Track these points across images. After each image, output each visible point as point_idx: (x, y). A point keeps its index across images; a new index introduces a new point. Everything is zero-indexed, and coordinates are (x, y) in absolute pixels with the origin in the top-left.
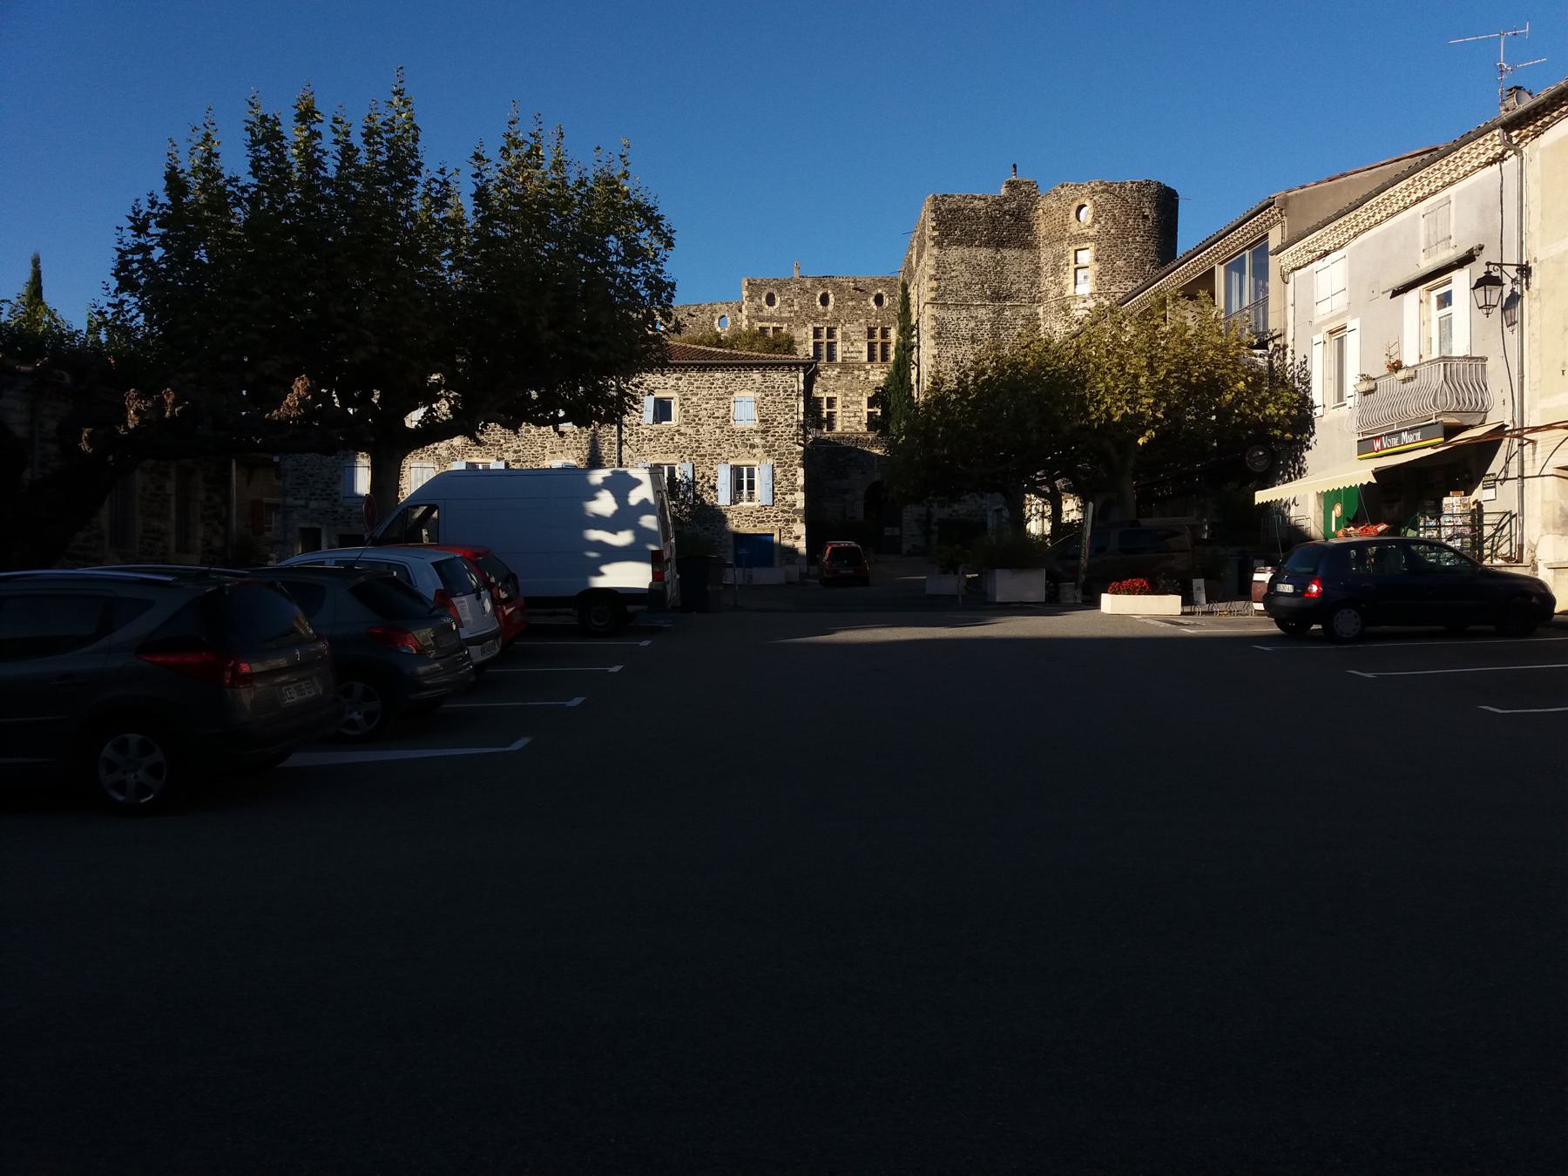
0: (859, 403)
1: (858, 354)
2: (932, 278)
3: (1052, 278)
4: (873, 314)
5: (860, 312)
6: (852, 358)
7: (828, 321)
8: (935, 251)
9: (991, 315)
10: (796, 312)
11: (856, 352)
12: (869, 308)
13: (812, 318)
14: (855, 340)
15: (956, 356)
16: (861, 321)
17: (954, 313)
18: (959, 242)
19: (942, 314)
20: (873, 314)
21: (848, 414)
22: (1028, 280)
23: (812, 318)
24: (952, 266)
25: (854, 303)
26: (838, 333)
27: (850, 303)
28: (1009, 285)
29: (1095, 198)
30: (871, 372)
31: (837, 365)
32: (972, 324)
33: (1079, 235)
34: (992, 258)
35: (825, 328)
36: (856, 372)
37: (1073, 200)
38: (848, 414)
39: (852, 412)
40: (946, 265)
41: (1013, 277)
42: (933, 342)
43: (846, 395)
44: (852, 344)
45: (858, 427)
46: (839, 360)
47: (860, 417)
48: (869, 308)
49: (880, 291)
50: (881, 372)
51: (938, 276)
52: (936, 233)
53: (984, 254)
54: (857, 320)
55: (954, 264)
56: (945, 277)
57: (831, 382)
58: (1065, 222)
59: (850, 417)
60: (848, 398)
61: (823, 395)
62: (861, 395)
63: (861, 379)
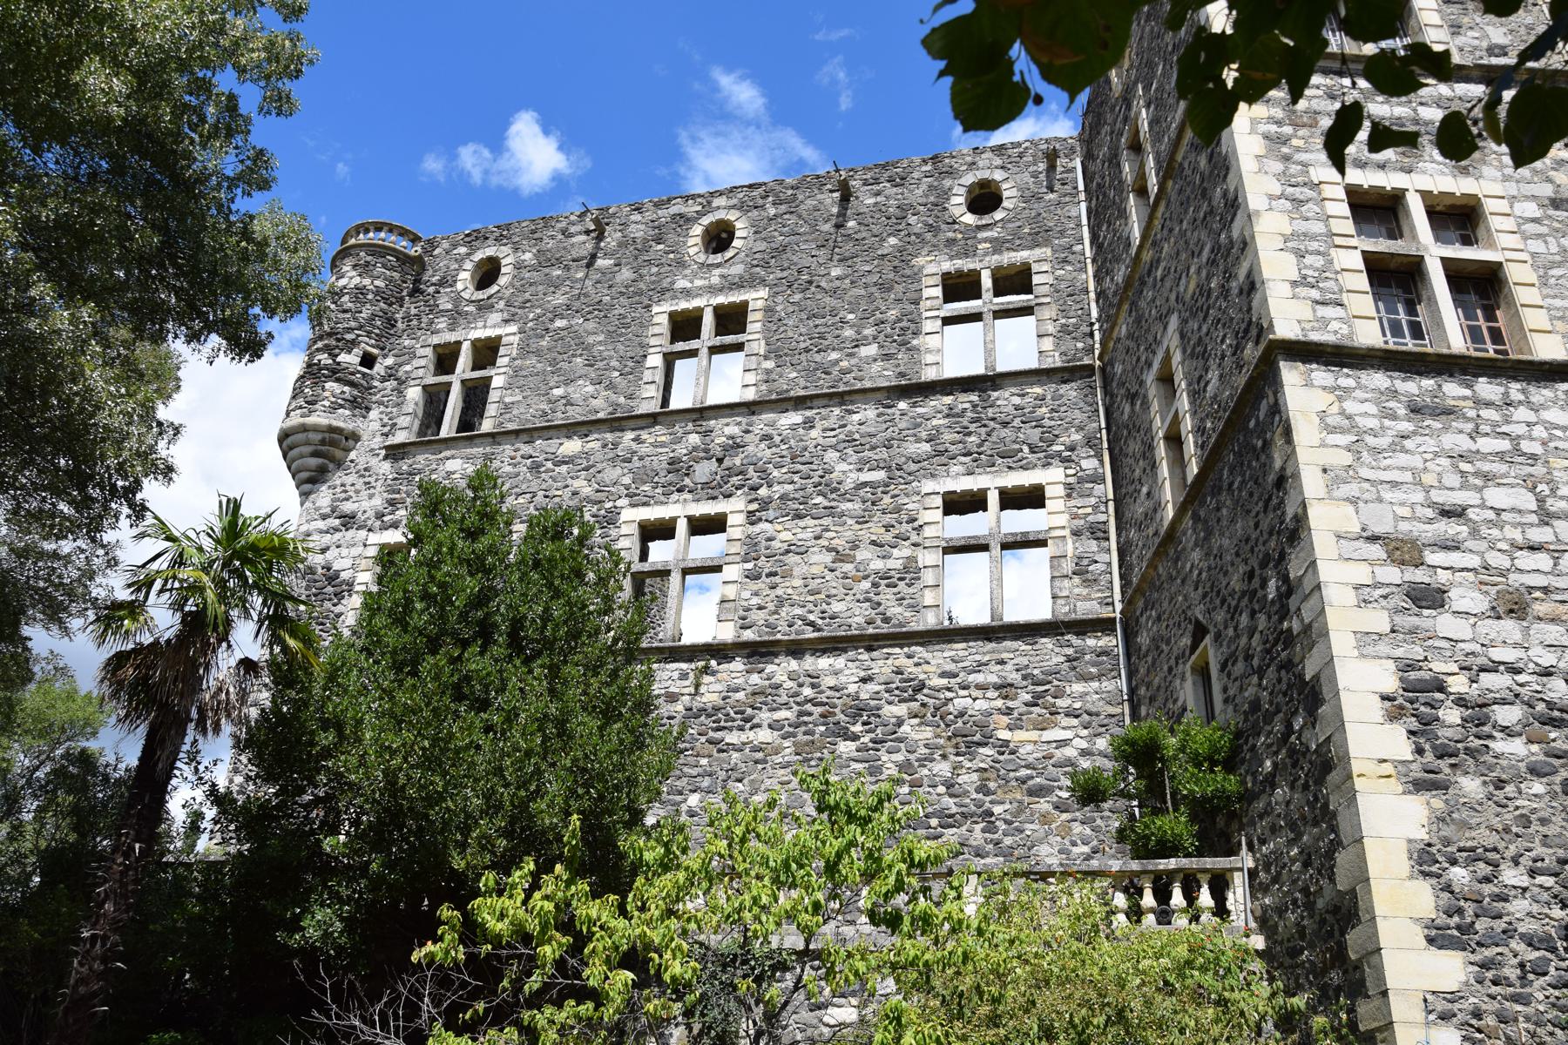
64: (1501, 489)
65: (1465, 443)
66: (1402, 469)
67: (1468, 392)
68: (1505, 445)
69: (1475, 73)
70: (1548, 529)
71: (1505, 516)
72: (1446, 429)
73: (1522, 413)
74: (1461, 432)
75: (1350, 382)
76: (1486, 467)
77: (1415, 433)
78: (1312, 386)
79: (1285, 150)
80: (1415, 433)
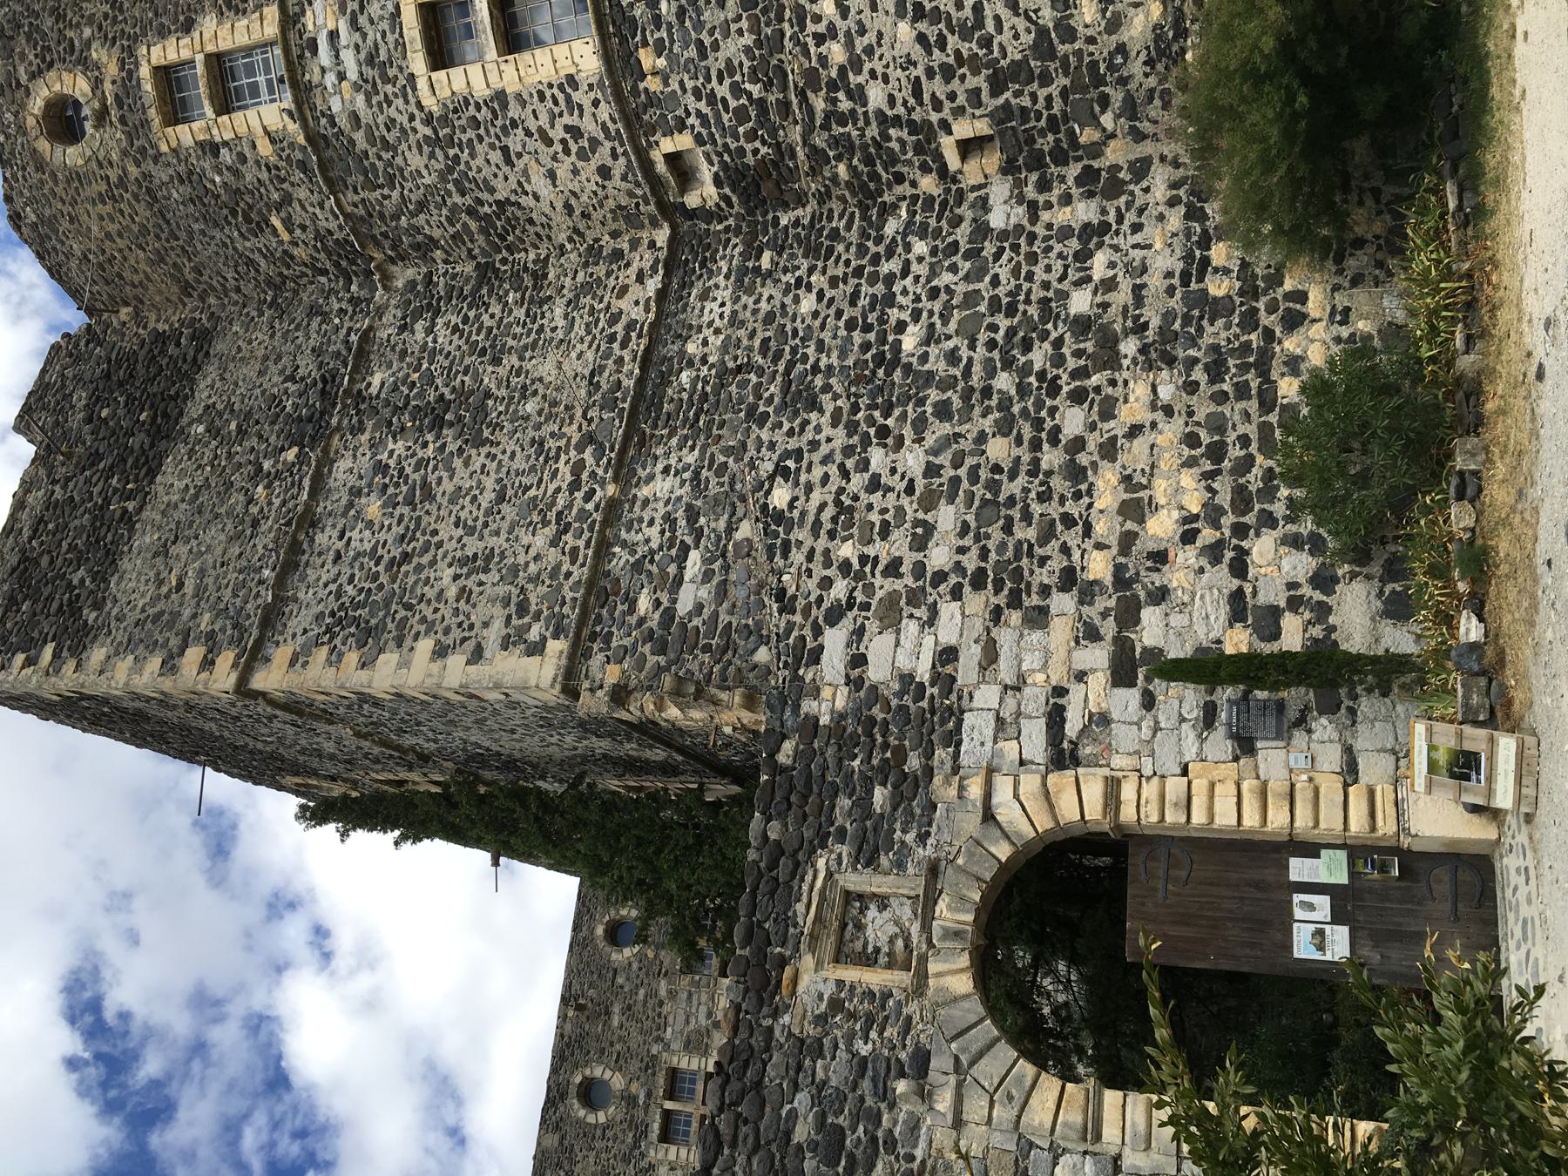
2: (170, 666)
3: (276, 221)
4: (651, 954)
5: (642, 992)
7: (649, 1095)
8: (97, 655)
9: (365, 438)
12: (635, 966)
13: (636, 1145)
14: (709, 1015)
15: (464, 561)
16: (663, 987)
17: (312, 578)
18: (107, 561)
19: (300, 620)
20: (651, 954)
22: (297, 329)
23: (636, 1145)
24: (164, 590)
25: (616, 1009)
27: (615, 1022)
28: (292, 388)
29: (23, 78)
32: (373, 507)
33: (123, 120)
34: (191, 452)
35: (669, 1105)
37: (40, 166)
40: (151, 611)
41: (274, 381)
42: (388, 660)
48: (635, 966)
49: (600, 930)
51: (174, 642)
52: (48, 652)
53: (173, 480)
54: (661, 1004)
55: (161, 583)
56: (187, 613)
58: (103, 187)
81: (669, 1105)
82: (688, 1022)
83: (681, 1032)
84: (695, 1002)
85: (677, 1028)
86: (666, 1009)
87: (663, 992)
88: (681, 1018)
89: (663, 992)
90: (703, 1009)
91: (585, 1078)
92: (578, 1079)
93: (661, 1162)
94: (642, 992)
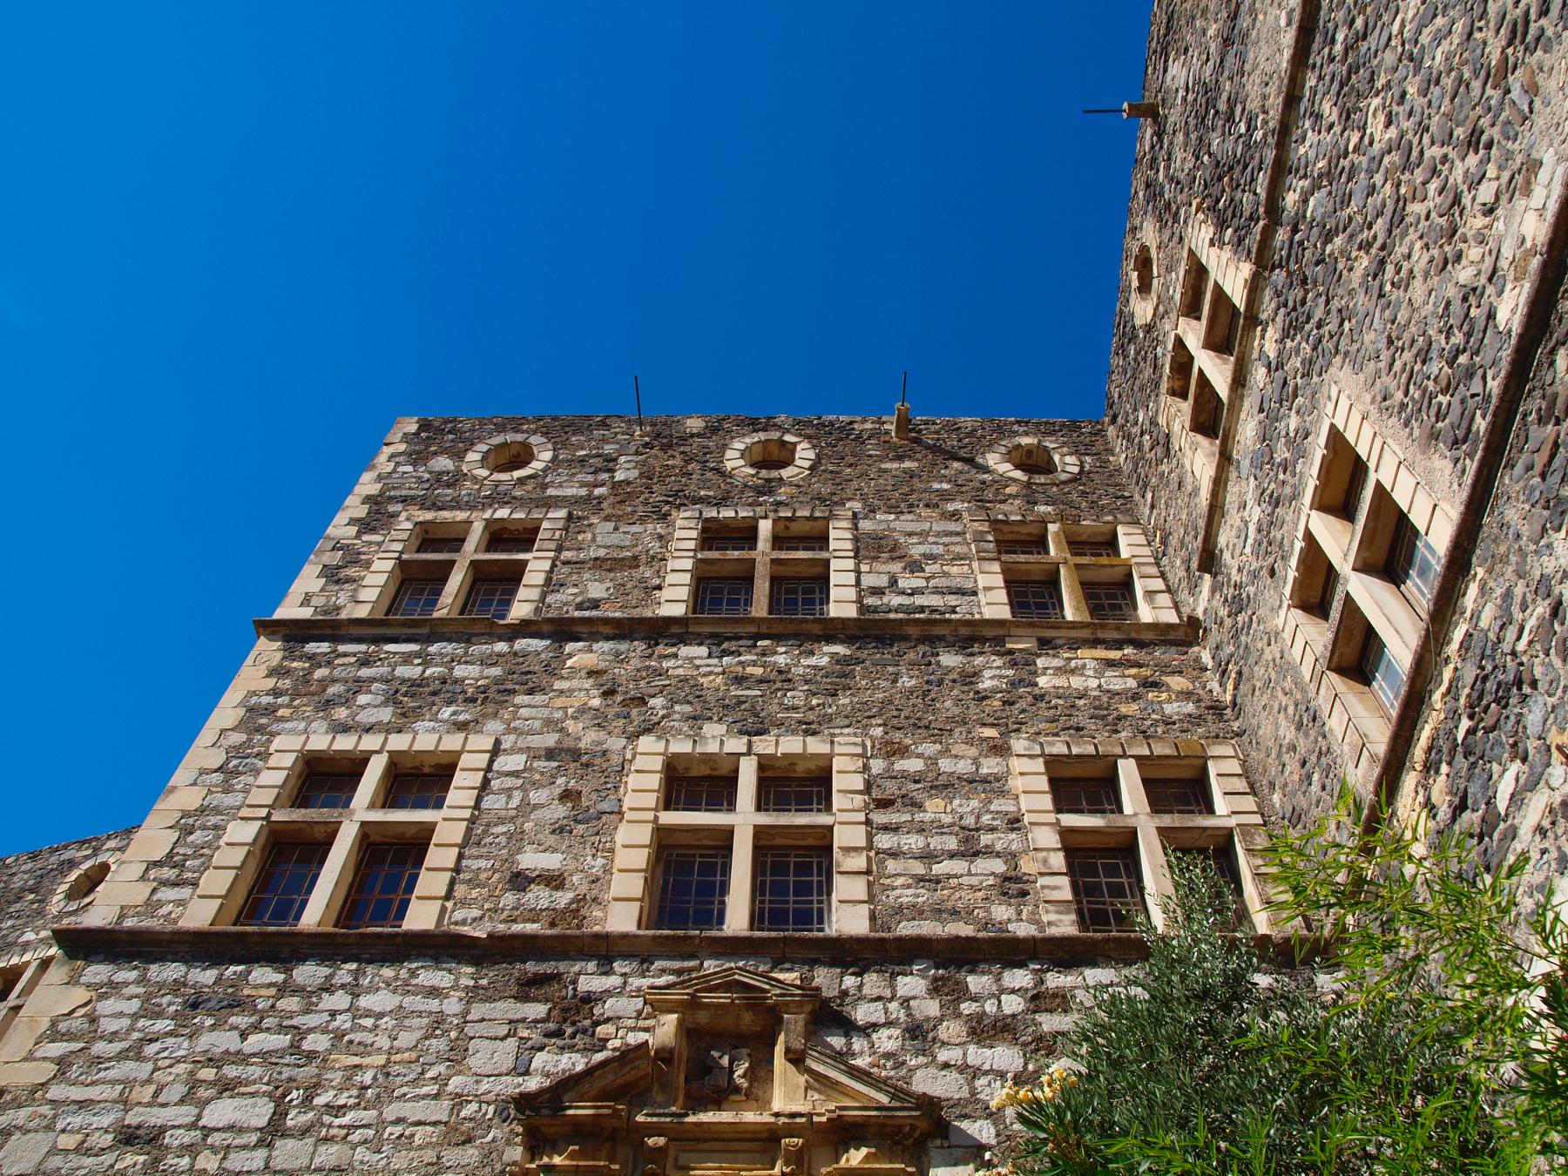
0: (994, 785)
1: (952, 600)
5: (945, 486)
6: (922, 609)
7: (779, 503)
10: (616, 485)
11: (937, 591)
14: (933, 557)
21: (914, 842)
23: (696, 500)
26: (840, 537)
30: (1041, 662)
31: (834, 631)
35: (765, 527)
36: (949, 659)
38: (914, 842)
39: (941, 829)
43: (895, 751)
44: (914, 567)
45: (1001, 912)
46: (841, 604)
47: (1011, 857)
50: (1111, 664)
57: (796, 697)
59: (928, 857)
60: (913, 765)
61: (736, 744)
62: (1000, 749)
63: (986, 684)
64: (237, 1102)
65: (225, 1041)
66: (114, 1082)
67: (279, 977)
68: (284, 1040)
69: (546, 629)
70: (261, 1153)
71: (214, 1139)
72: (213, 1027)
73: (340, 1000)
74: (236, 1028)
75: (133, 975)
76: (231, 1071)
77: (170, 1034)
78: (77, 983)
79: (263, 721)
80: (170, 1034)
81: (765, 527)
82: (910, 534)
83: (889, 529)
84: (946, 540)
85: (897, 525)
86: (925, 512)
87: (951, 507)
88: (910, 527)
89: (951, 507)
90: (939, 550)
91: (795, 444)
92: (789, 438)
93: (672, 525)
94: (945, 486)
